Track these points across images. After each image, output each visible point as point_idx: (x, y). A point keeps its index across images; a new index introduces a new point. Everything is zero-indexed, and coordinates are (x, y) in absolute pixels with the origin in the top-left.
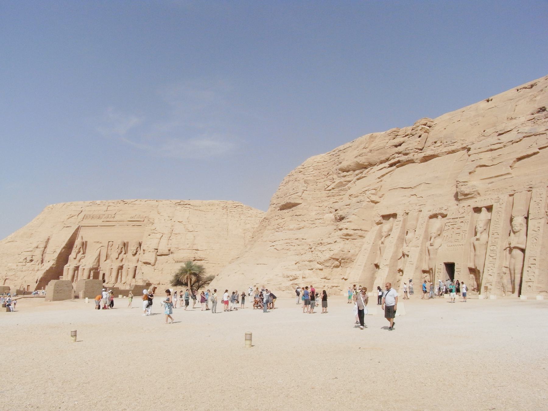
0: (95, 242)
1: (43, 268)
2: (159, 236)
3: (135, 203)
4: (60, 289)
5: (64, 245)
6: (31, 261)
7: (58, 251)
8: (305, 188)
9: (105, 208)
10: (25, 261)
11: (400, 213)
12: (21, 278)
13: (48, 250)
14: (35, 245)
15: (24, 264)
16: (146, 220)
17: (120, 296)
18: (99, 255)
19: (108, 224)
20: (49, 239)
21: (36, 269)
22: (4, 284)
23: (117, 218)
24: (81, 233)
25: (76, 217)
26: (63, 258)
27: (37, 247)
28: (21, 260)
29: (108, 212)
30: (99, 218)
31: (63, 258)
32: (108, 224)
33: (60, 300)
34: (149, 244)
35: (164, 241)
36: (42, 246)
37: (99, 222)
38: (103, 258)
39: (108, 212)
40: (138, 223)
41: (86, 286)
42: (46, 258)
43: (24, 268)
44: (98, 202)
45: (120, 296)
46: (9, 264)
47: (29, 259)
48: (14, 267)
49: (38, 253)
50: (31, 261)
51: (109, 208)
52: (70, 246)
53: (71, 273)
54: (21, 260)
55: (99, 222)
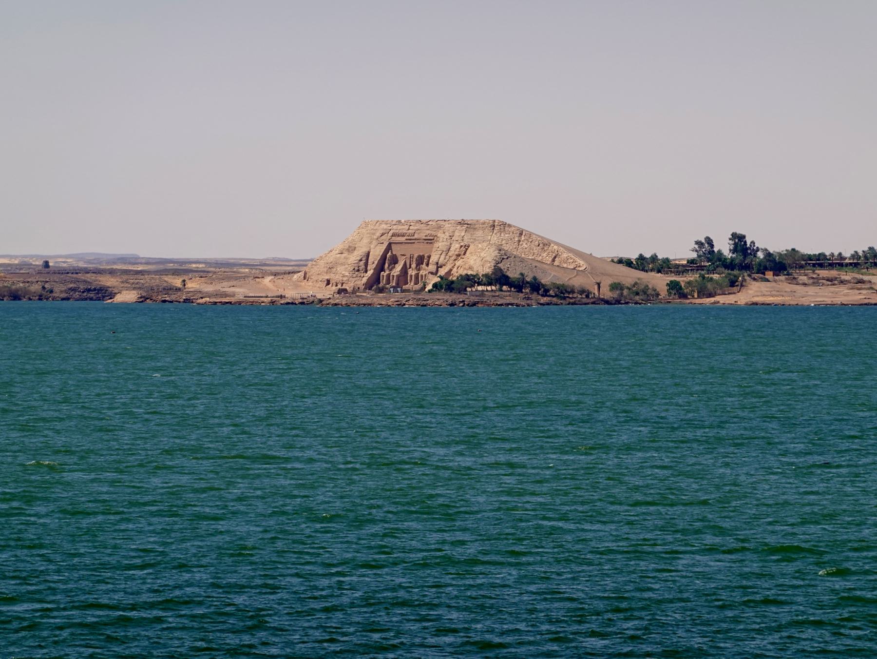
2: (440, 252)
7: (376, 262)
18: (405, 264)
20: (368, 255)
23: (416, 236)
27: (361, 260)
29: (410, 231)
30: (403, 236)
31: (381, 268)
34: (434, 259)
35: (443, 257)
37: (403, 239)
39: (410, 231)
42: (369, 268)
52: (383, 258)
55: (403, 239)
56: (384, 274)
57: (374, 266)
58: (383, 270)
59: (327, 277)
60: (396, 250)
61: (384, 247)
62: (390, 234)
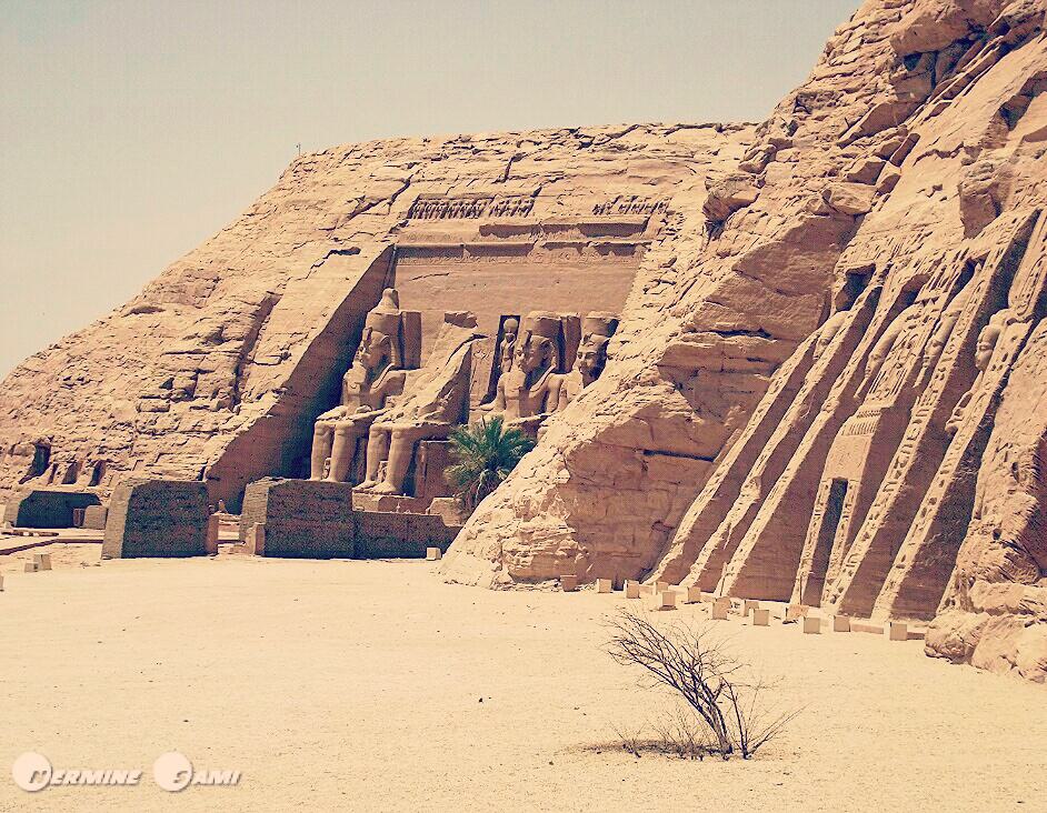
0: (449, 319)
1: (237, 420)
3: (622, 141)
4: (154, 513)
6: (189, 394)
7: (298, 352)
8: (782, 134)
9: (496, 165)
10: (167, 392)
11: (879, 270)
12: (147, 459)
13: (265, 349)
14: (206, 329)
15: (163, 403)
16: (656, 221)
17: (432, 552)
18: (464, 374)
20: (269, 303)
21: (207, 428)
22: (96, 480)
23: (542, 213)
25: (382, 208)
27: (218, 338)
28: (153, 389)
30: (473, 212)
31: (320, 384)
33: (358, 554)
38: (479, 389)
39: (512, 186)
41: (271, 504)
43: (164, 421)
45: (432, 552)
46: (119, 404)
47: (181, 382)
48: (131, 416)
49: (220, 361)
50: (189, 394)
52: (345, 331)
55: (463, 230)
56: (339, 418)
57: (287, 369)
58: (334, 397)
59: (40, 432)
60: (417, 289)
61: (357, 268)
62: (402, 204)
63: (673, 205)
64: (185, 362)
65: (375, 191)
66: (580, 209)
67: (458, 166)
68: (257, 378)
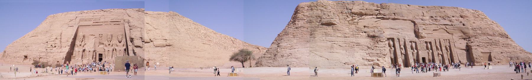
5: (73, 37)
19: (97, 24)
23: (102, 20)
24: (80, 30)
26: (73, 45)
31: (73, 45)
32: (97, 24)
36: (59, 38)
40: (117, 23)
44: (86, 11)
47: (54, 45)
49: (58, 41)
51: (95, 15)
53: (81, 53)
54: (49, 46)
55: (91, 23)
62: (78, 20)
63: (125, 19)
64: (53, 42)
65: (72, 18)
66: (109, 19)
67: (84, 15)
68: (63, 45)
